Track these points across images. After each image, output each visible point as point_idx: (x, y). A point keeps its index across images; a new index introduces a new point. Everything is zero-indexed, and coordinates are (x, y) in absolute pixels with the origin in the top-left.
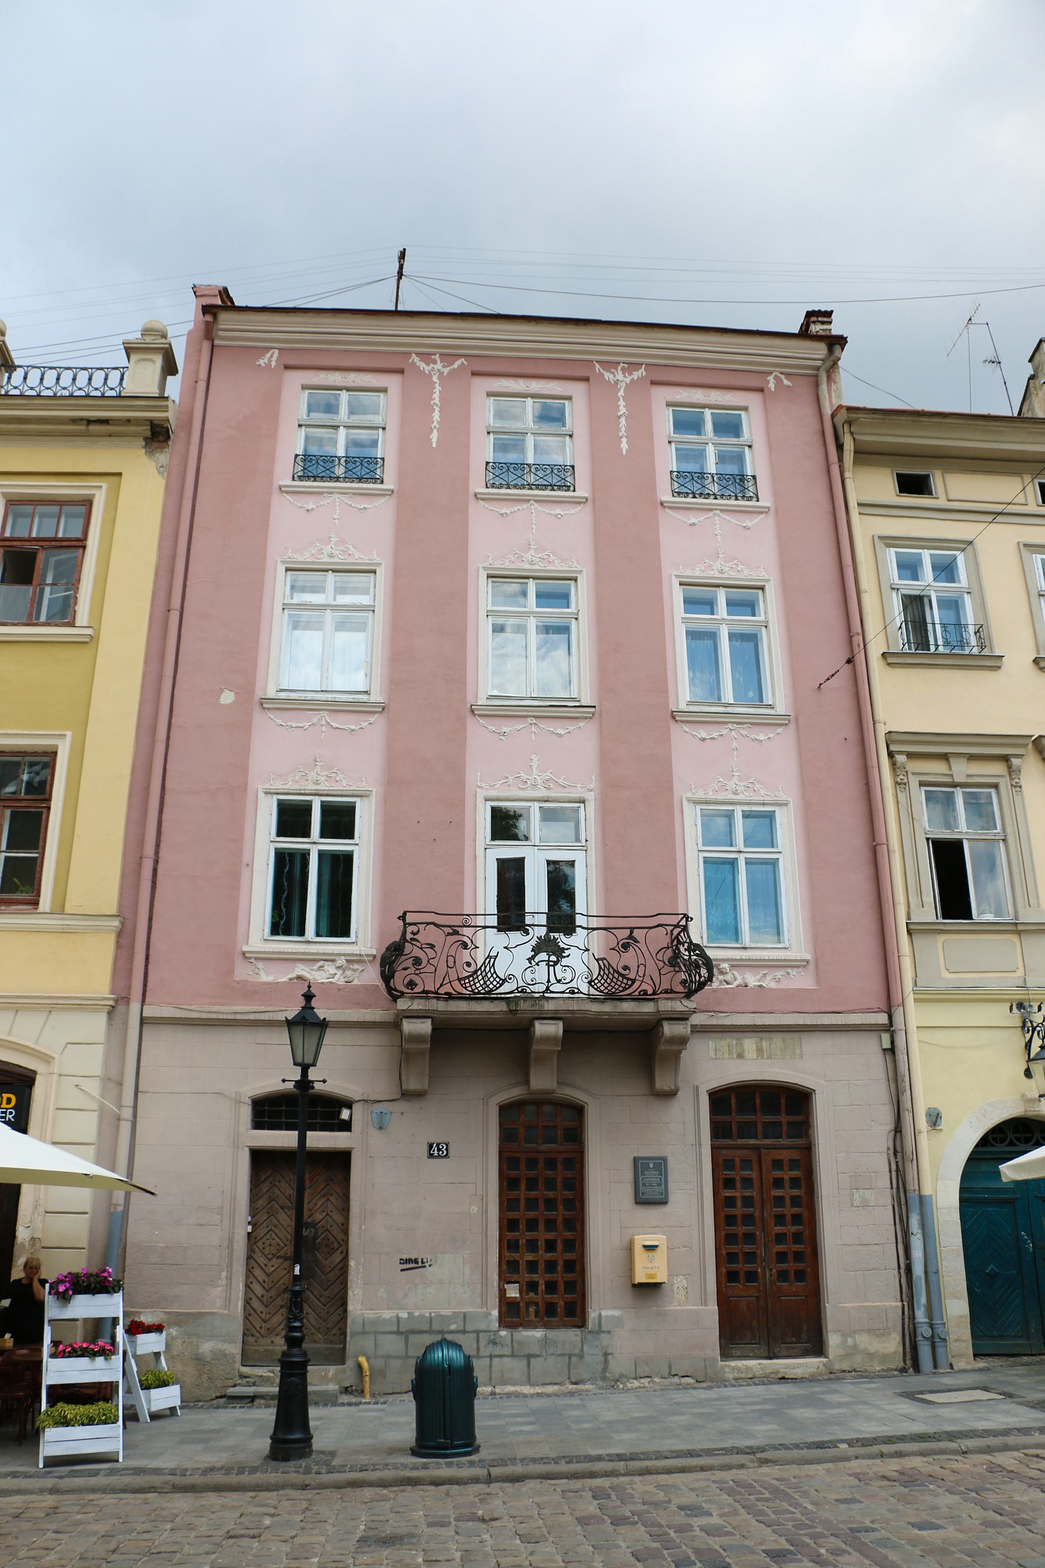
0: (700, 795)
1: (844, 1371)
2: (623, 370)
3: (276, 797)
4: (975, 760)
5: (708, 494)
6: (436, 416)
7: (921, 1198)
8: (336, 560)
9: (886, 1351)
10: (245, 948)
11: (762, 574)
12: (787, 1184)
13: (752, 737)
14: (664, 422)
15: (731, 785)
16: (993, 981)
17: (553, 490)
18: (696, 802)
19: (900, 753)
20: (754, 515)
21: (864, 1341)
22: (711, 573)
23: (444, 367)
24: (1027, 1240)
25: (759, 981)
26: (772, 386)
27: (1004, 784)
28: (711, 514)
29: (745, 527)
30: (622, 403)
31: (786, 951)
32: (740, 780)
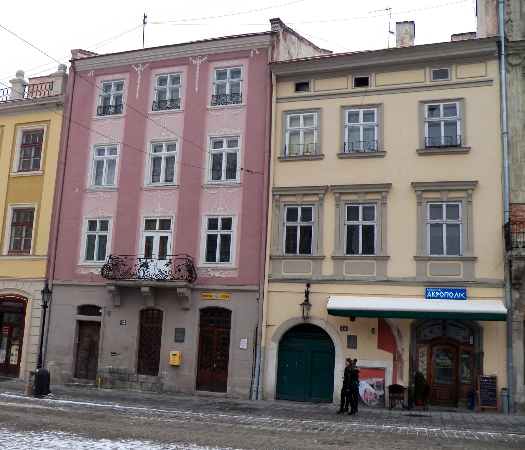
0: (208, 213)
2: (200, 58)
3: (88, 219)
6: (138, 87)
8: (108, 142)
10: (78, 264)
13: (228, 192)
14: (213, 76)
17: (173, 109)
18: (207, 215)
19: (277, 195)
22: (221, 133)
23: (142, 68)
26: (252, 55)
28: (224, 110)
30: (198, 72)
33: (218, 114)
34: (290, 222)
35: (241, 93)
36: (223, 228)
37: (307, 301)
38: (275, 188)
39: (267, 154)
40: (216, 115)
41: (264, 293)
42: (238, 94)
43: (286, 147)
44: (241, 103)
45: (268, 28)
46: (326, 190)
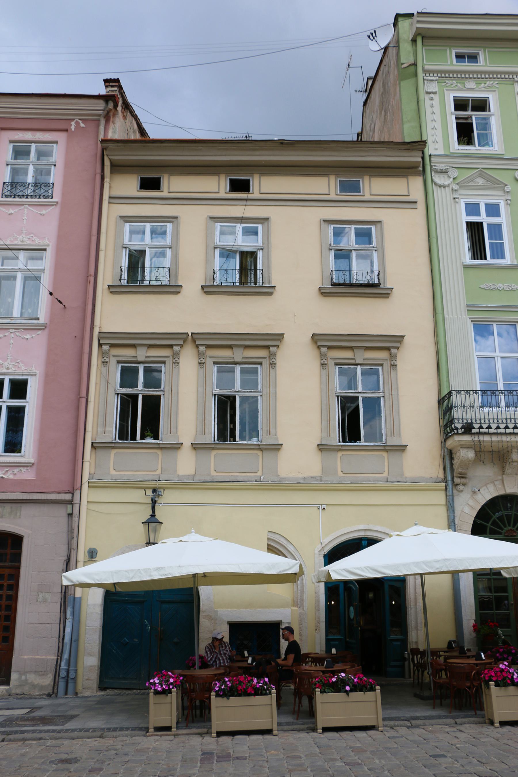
1: (18, 694)
4: (153, 347)
5: (23, 196)
7: (74, 598)
9: (44, 684)
11: (46, 242)
12: (5, 588)
13: (22, 337)
15: (6, 364)
16: (141, 476)
19: (106, 344)
20: (49, 207)
21: (32, 678)
22: (16, 242)
24: (147, 625)
25: (4, 474)
26: (73, 128)
27: (169, 361)
28: (23, 207)
29: (41, 214)
31: (22, 457)
32: (11, 361)
33: (11, 211)
34: (126, 389)
35: (53, 184)
36: (12, 396)
37: (153, 515)
38: (103, 333)
39: (92, 279)
40: (10, 212)
41: (80, 504)
42: (47, 184)
43: (122, 271)
44: (52, 198)
45: (102, 91)
46: (185, 341)
